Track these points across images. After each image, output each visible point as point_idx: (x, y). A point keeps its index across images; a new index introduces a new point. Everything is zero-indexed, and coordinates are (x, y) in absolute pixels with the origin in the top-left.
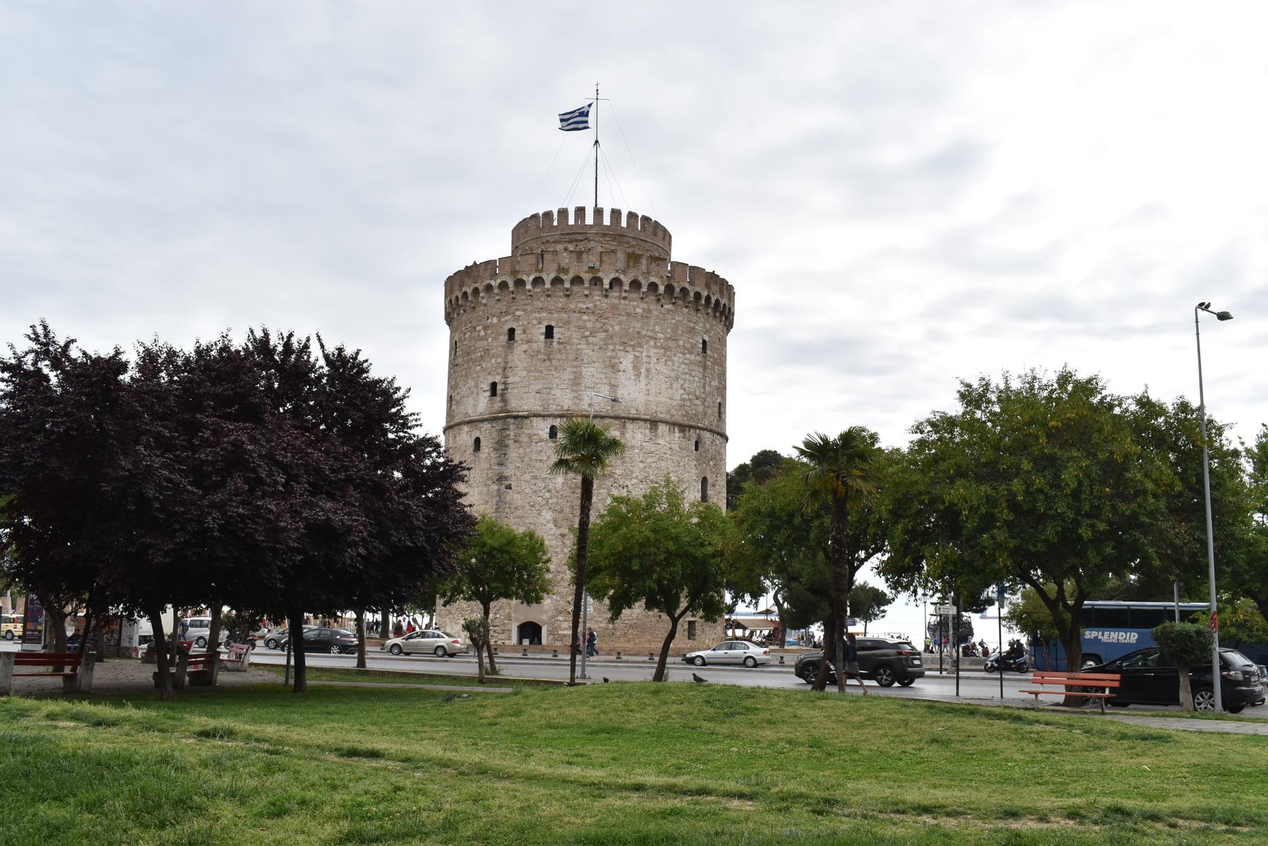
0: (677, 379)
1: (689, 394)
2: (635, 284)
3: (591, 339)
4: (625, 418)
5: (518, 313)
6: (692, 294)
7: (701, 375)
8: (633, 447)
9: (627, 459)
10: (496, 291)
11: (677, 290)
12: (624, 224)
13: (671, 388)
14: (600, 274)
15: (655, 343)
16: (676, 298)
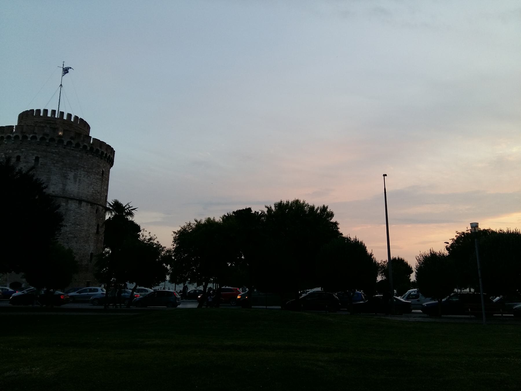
0: (91, 184)
1: (95, 191)
2: (78, 145)
3: (56, 165)
4: (68, 198)
5: (22, 150)
6: (100, 152)
7: (100, 184)
8: (71, 210)
10: (13, 139)
11: (95, 150)
12: (72, 120)
13: (89, 188)
14: (63, 139)
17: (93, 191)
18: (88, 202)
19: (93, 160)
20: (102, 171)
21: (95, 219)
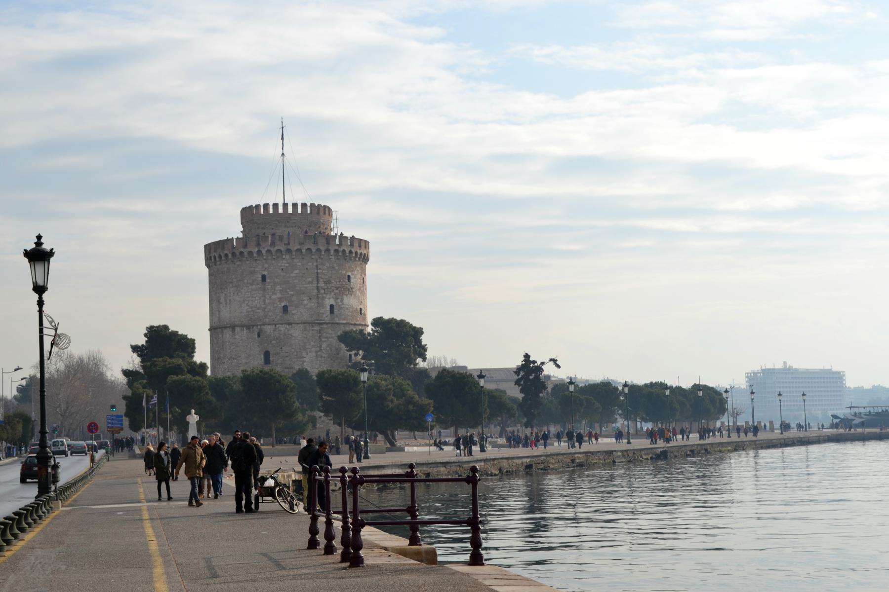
0: (244, 301)
1: (252, 308)
2: (220, 256)
4: (223, 327)
7: (261, 295)
9: (225, 349)
11: (238, 254)
13: (241, 307)
15: (232, 285)
16: (239, 258)
17: (248, 309)
18: (242, 326)
19: (242, 268)
20: (261, 276)
21: (258, 346)
